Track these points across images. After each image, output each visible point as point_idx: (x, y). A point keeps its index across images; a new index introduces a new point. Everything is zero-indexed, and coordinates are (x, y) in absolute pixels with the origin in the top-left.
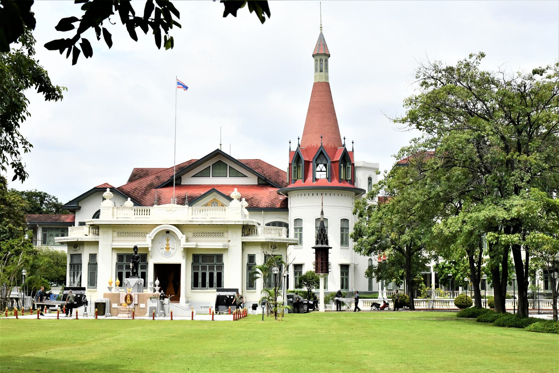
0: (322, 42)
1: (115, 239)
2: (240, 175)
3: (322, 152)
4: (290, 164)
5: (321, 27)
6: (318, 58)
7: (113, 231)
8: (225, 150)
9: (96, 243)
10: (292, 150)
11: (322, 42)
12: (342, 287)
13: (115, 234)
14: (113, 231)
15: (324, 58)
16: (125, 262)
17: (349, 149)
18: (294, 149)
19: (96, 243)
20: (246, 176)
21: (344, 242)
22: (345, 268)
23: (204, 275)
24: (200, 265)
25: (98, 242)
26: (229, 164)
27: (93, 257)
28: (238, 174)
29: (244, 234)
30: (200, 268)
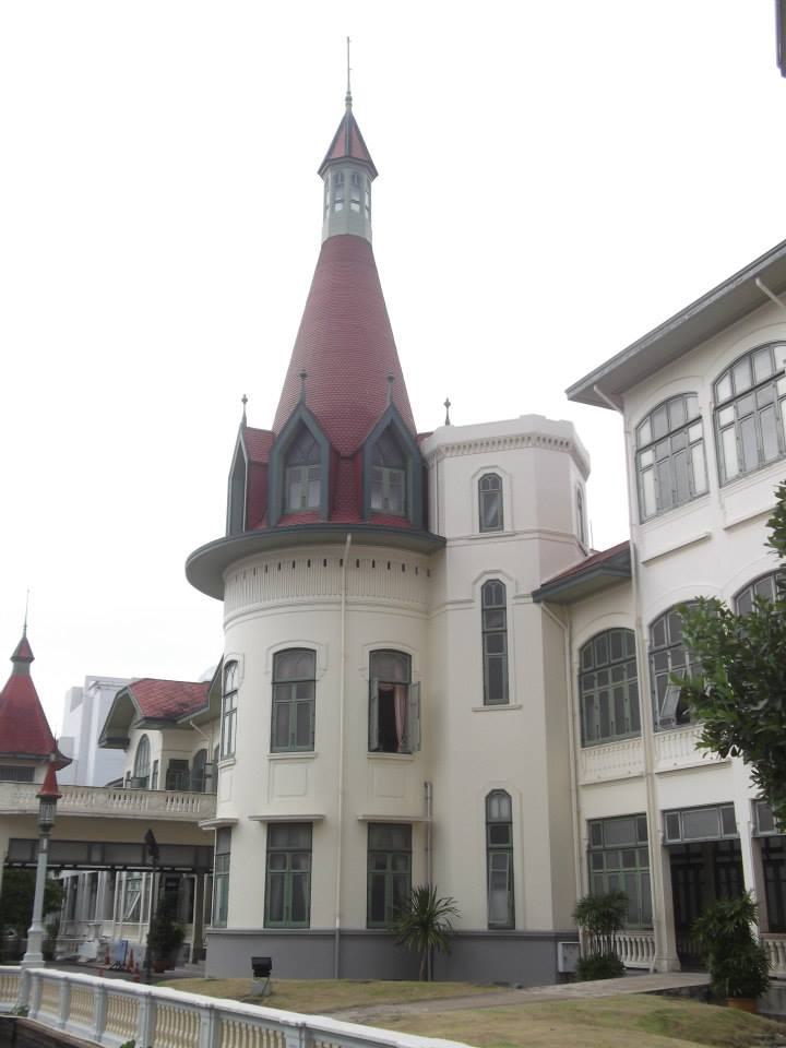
5: (349, 100)
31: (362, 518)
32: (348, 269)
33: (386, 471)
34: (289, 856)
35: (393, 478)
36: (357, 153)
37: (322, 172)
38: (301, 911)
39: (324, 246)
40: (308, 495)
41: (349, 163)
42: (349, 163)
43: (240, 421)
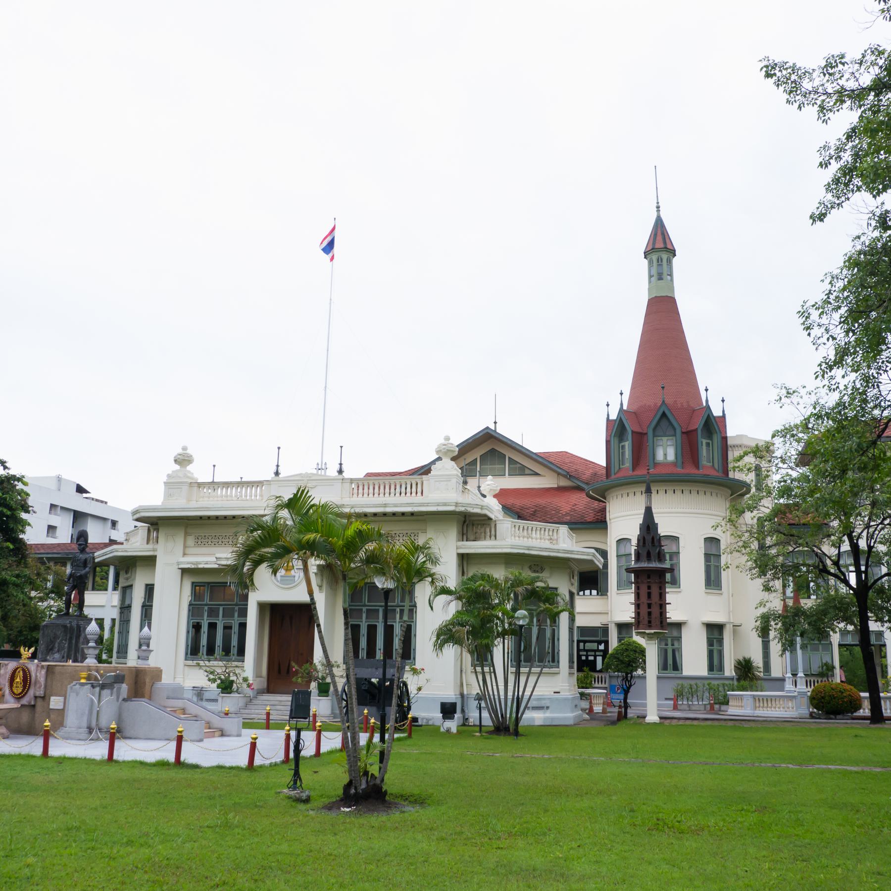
0: (659, 230)
1: (188, 551)
2: (527, 471)
3: (664, 415)
4: (608, 443)
5: (658, 207)
6: (654, 257)
7: (186, 534)
8: (504, 430)
9: (150, 561)
10: (611, 418)
11: (659, 230)
12: (711, 668)
13: (191, 541)
14: (186, 534)
15: (665, 256)
16: (207, 600)
17: (717, 412)
18: (614, 416)
19: (150, 561)
20: (537, 474)
21: (713, 580)
22: (715, 631)
23: (372, 629)
24: (364, 609)
25: (156, 557)
26: (509, 454)
27: (150, 589)
28: (521, 471)
29: (464, 535)
30: (364, 615)
31: (697, 467)
32: (663, 315)
33: (704, 441)
34: (669, 640)
35: (708, 444)
36: (669, 246)
37: (646, 254)
38: (676, 667)
39: (649, 300)
40: (666, 452)
41: (660, 248)
42: (660, 248)
43: (619, 407)
